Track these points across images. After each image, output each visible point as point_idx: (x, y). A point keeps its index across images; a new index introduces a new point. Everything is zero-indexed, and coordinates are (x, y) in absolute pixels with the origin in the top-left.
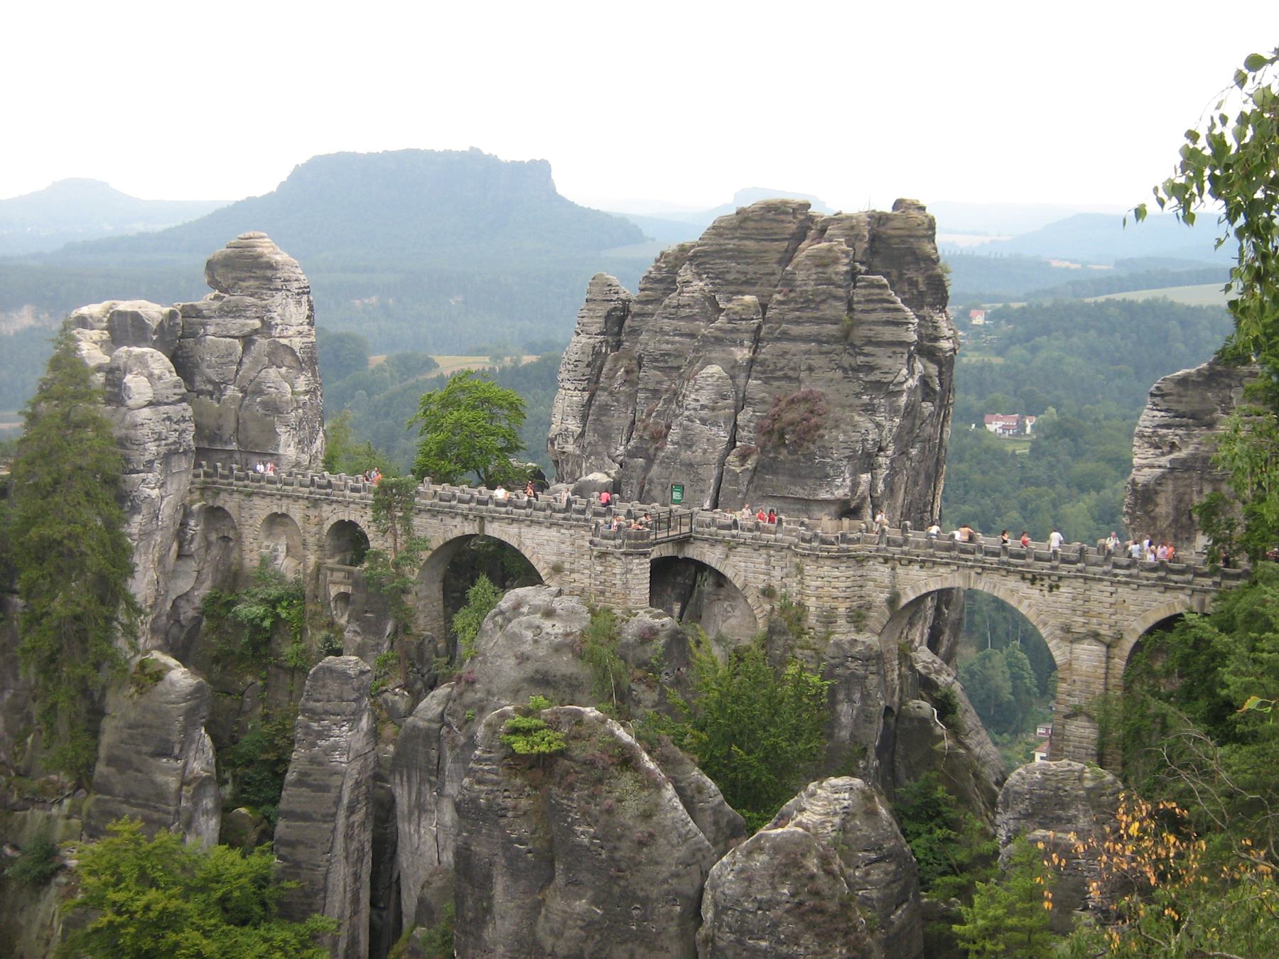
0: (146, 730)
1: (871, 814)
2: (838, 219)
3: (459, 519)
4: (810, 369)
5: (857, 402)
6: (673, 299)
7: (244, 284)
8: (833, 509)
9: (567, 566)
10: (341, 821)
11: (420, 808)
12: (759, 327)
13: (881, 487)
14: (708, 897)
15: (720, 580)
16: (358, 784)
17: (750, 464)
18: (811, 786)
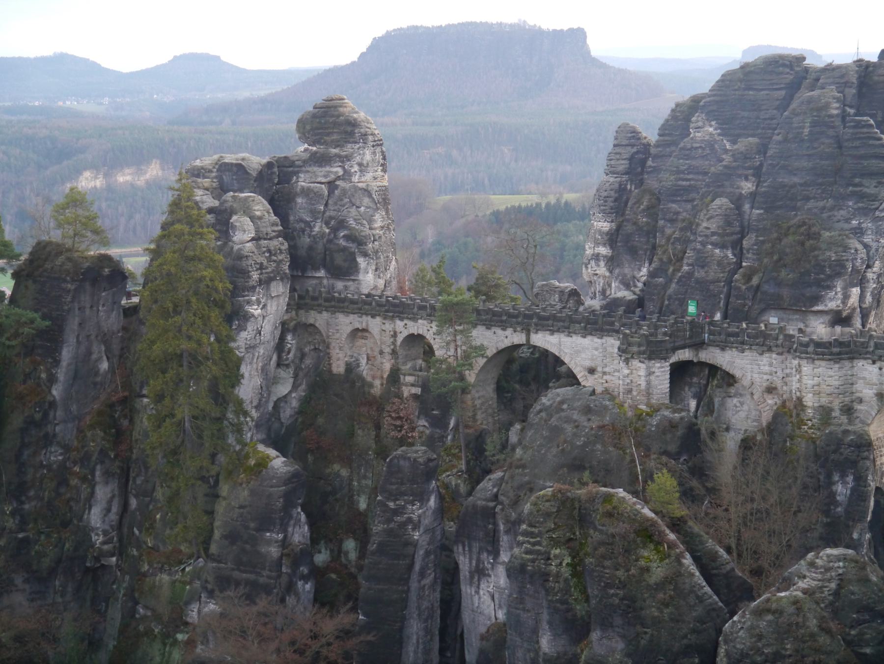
1: (866, 581)
2: (830, 69)
3: (509, 331)
5: (846, 226)
6: (686, 143)
8: (827, 318)
9: (599, 369)
10: (414, 585)
11: (480, 573)
12: (761, 165)
13: (869, 298)
14: (722, 651)
15: (729, 379)
16: (427, 553)
17: (755, 281)
18: (810, 556)
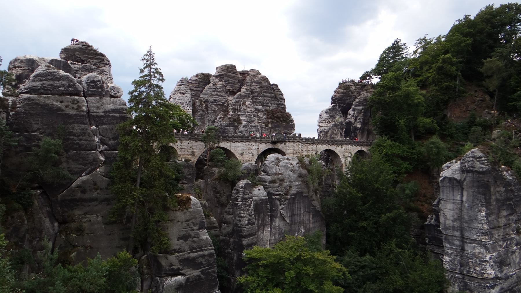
0: (194, 220)
4: (271, 104)
7: (91, 60)
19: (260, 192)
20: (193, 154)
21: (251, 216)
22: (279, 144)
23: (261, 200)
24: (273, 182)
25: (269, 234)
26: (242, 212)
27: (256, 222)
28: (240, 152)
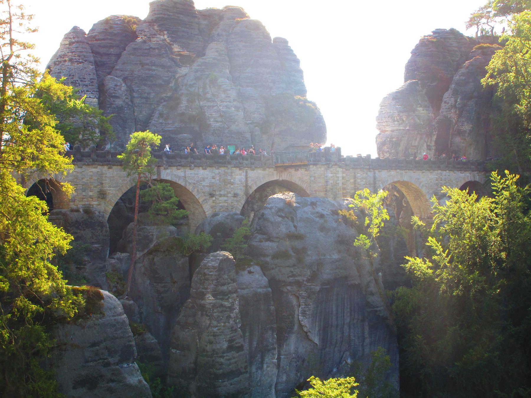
19: (254, 279)
20: (102, 195)
21: (236, 330)
22: (292, 171)
23: (256, 294)
24: (282, 255)
25: (275, 371)
26: (215, 323)
27: (246, 346)
28: (207, 189)
